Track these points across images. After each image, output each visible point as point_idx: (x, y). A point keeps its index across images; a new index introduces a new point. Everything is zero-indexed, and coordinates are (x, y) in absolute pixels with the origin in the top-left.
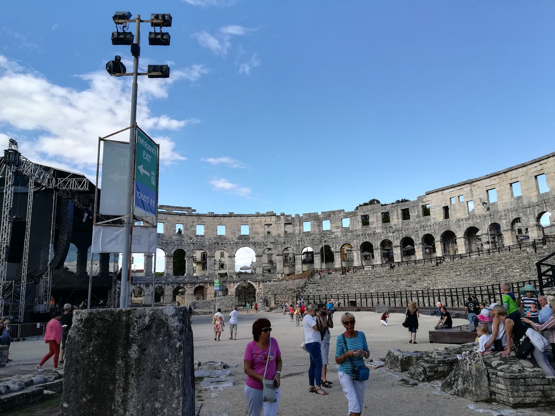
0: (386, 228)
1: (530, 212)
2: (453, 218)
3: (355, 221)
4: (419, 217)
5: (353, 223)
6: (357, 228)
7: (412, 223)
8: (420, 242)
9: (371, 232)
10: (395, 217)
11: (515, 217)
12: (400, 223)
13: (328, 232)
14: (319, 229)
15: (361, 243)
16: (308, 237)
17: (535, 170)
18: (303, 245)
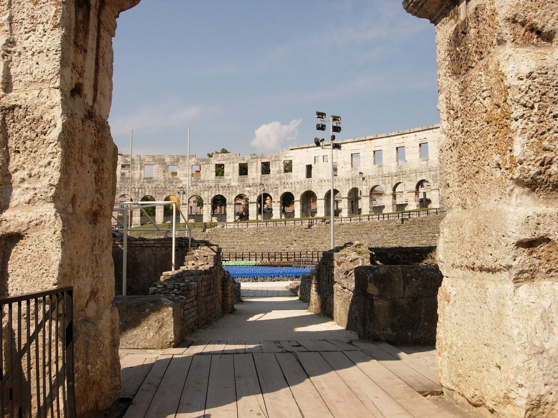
0: (243, 181)
1: (388, 181)
2: (316, 178)
3: (207, 170)
4: (281, 173)
5: (205, 172)
6: (210, 179)
7: (272, 178)
8: (279, 200)
9: (225, 184)
10: (254, 170)
11: (375, 184)
12: (259, 177)
13: (175, 180)
14: (164, 175)
15: (213, 196)
16: (150, 184)
17: (397, 141)
18: (143, 193)
